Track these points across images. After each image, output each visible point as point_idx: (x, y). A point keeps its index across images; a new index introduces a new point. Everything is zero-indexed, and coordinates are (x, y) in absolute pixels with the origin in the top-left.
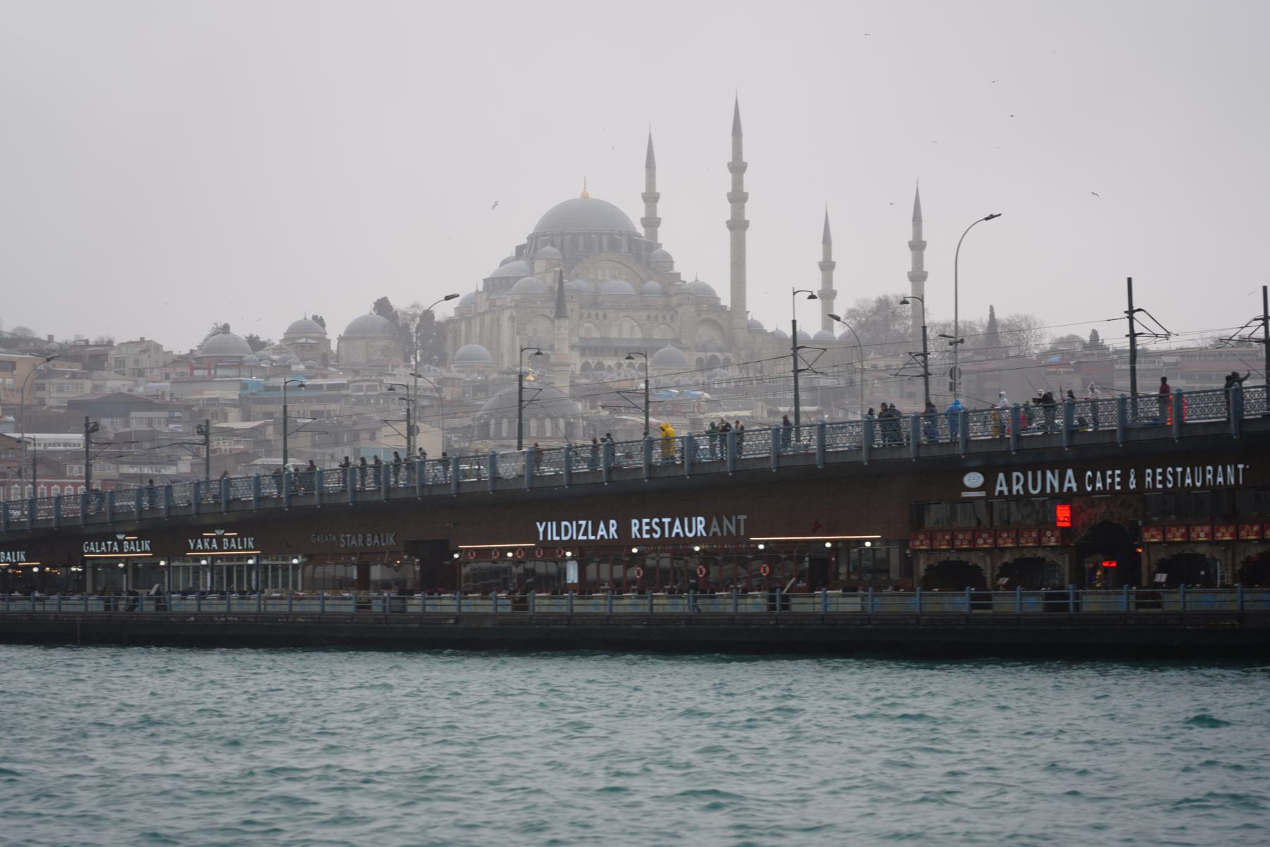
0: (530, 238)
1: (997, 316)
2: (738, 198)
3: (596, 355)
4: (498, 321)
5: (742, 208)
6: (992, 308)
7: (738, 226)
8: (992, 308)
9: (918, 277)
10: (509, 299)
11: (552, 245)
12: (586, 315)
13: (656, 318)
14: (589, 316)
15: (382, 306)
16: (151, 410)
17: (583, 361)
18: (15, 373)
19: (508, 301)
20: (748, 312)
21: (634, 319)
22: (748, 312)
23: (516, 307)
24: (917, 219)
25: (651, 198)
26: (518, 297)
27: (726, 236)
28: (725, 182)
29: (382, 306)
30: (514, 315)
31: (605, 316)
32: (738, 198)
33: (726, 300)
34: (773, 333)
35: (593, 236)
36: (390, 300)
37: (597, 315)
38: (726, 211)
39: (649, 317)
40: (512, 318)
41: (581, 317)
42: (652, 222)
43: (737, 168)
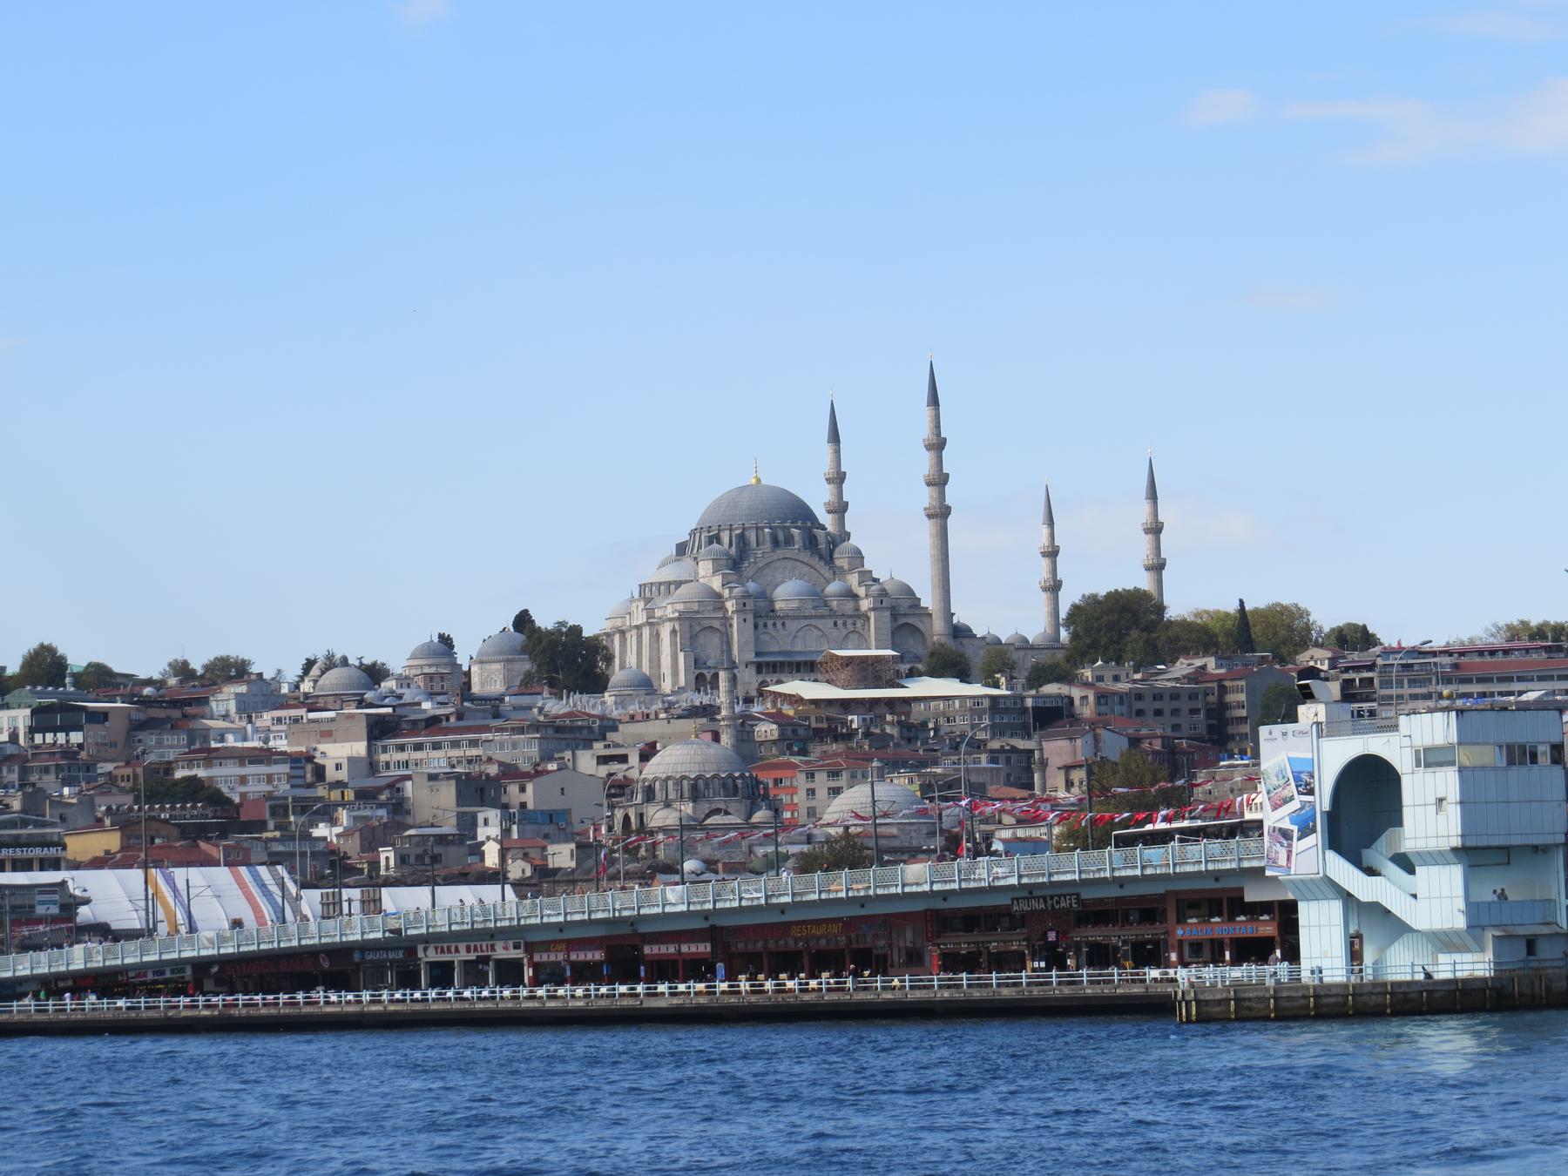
0: (693, 533)
1: (1248, 607)
2: (939, 481)
3: (774, 672)
4: (658, 635)
5: (942, 495)
6: (1242, 602)
7: (940, 513)
8: (1242, 602)
9: (1157, 567)
10: (670, 608)
11: (719, 542)
12: (761, 625)
13: (845, 624)
14: (765, 625)
15: (523, 621)
16: (269, 763)
17: (760, 680)
18: (107, 724)
19: (670, 612)
20: (953, 614)
21: (816, 628)
22: (953, 614)
23: (678, 619)
24: (1153, 495)
25: (838, 479)
26: (681, 607)
27: (927, 528)
28: (923, 463)
29: (523, 621)
30: (677, 627)
31: (784, 624)
32: (939, 481)
33: (928, 599)
34: (983, 638)
35: (767, 530)
36: (531, 613)
37: (774, 624)
38: (925, 496)
39: (835, 624)
40: (674, 632)
41: (756, 626)
42: (839, 509)
43: (937, 445)
